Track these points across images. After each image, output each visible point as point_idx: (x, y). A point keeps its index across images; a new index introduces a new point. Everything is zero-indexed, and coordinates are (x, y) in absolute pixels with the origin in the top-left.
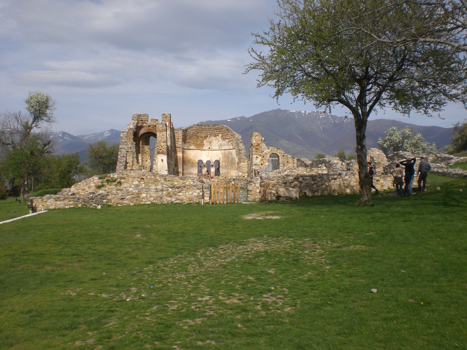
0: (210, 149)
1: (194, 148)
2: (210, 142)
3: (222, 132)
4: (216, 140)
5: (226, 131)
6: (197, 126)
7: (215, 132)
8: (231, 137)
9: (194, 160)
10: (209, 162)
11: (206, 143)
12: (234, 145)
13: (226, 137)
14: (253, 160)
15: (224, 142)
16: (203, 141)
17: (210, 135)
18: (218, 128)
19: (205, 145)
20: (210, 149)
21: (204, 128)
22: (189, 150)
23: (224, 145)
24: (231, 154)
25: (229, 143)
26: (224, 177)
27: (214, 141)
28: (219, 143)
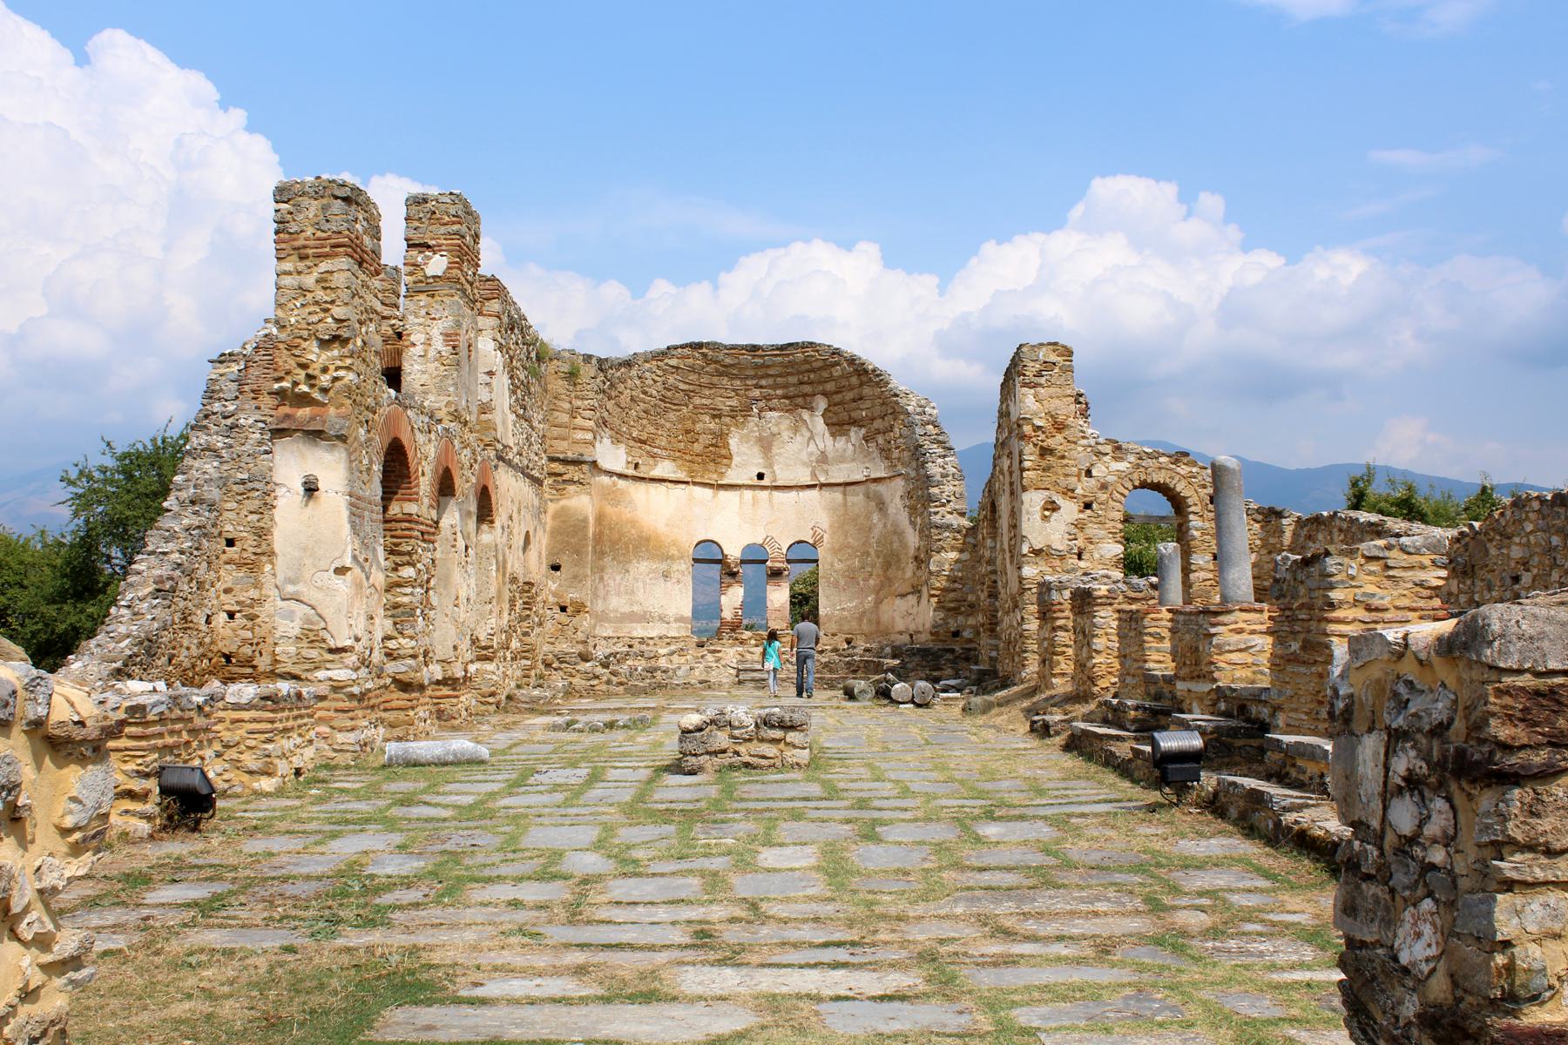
0: (763, 483)
1: (673, 476)
2: (766, 444)
3: (830, 387)
4: (796, 430)
5: (854, 380)
6: (687, 351)
7: (785, 386)
8: (877, 410)
9: (674, 543)
10: (755, 557)
12: (896, 454)
13: (854, 414)
15: (841, 443)
16: (720, 438)
17: (761, 404)
18: (806, 361)
19: (736, 459)
20: (766, 482)
21: (728, 361)
22: (642, 486)
23: (841, 459)
27: (786, 435)
28: (812, 447)
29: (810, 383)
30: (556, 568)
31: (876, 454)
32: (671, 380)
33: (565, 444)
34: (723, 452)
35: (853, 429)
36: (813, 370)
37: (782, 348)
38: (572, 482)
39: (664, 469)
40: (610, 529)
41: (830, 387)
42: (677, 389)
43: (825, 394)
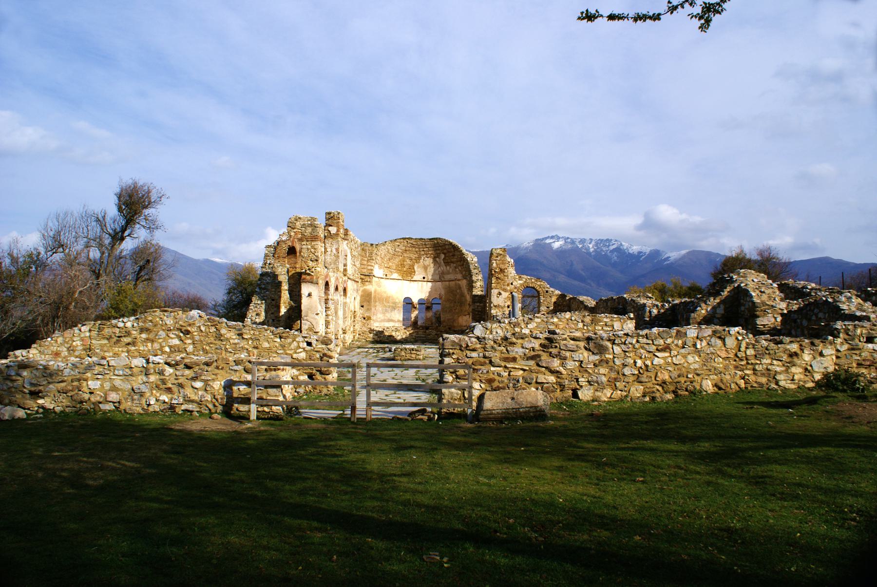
6: (402, 240)
11: (419, 270)
13: (453, 260)
14: (492, 299)
15: (448, 267)
16: (413, 266)
17: (424, 256)
19: (416, 273)
20: (425, 280)
21: (414, 243)
23: (449, 273)
24: (460, 288)
25: (457, 270)
26: (447, 327)
29: (439, 250)
30: (362, 306)
31: (458, 272)
32: (397, 249)
33: (365, 270)
34: (413, 270)
35: (452, 264)
36: (440, 246)
37: (430, 239)
38: (367, 281)
39: (395, 276)
40: (378, 294)
41: (445, 251)
42: (399, 252)
43: (443, 253)
